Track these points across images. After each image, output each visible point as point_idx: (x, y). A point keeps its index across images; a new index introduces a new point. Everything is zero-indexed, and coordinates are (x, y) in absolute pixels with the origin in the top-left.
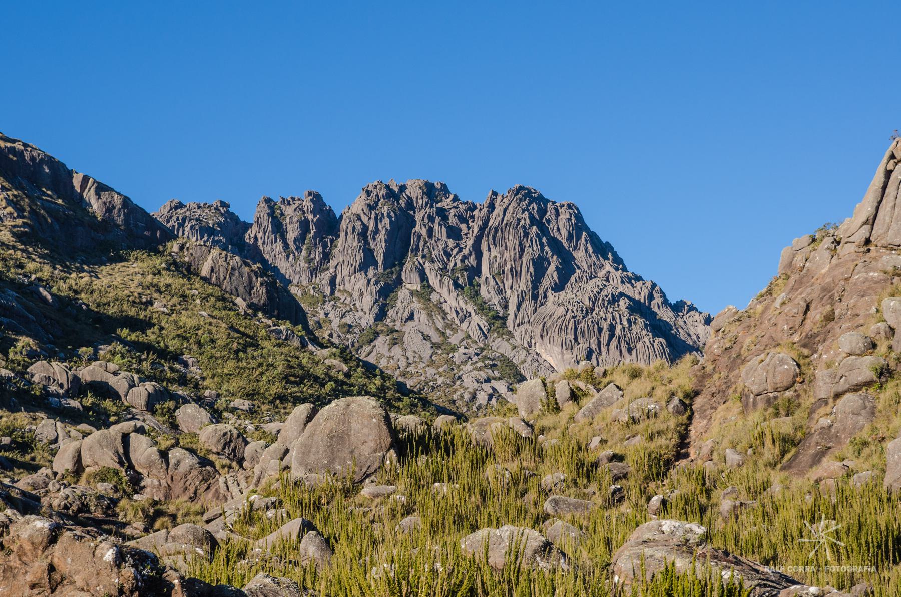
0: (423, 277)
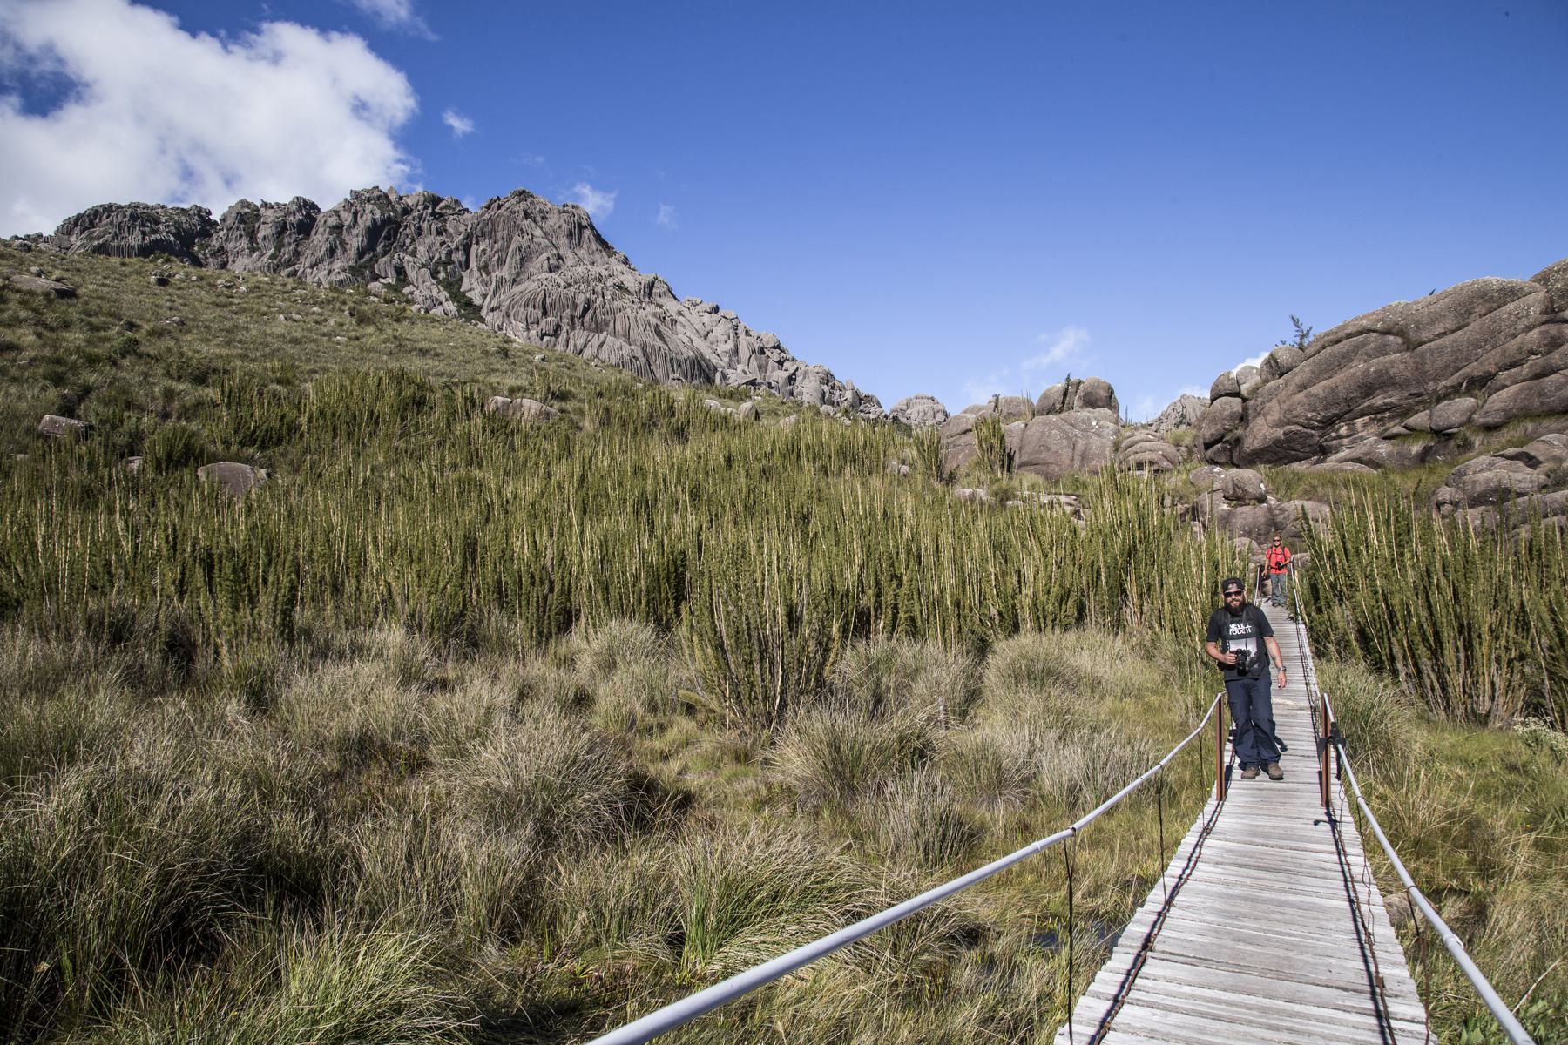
0: (400, 271)
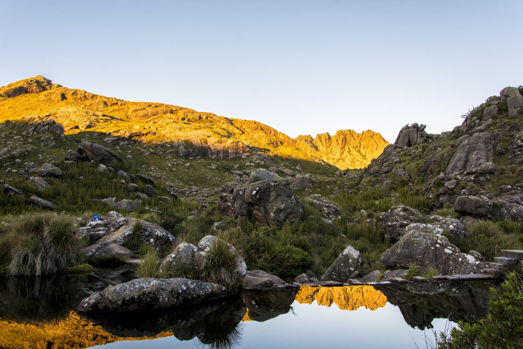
0: (349, 148)
